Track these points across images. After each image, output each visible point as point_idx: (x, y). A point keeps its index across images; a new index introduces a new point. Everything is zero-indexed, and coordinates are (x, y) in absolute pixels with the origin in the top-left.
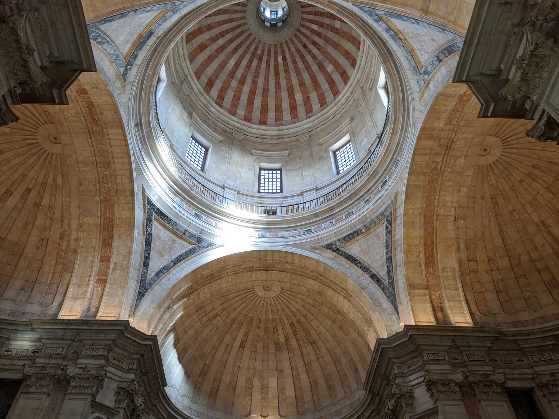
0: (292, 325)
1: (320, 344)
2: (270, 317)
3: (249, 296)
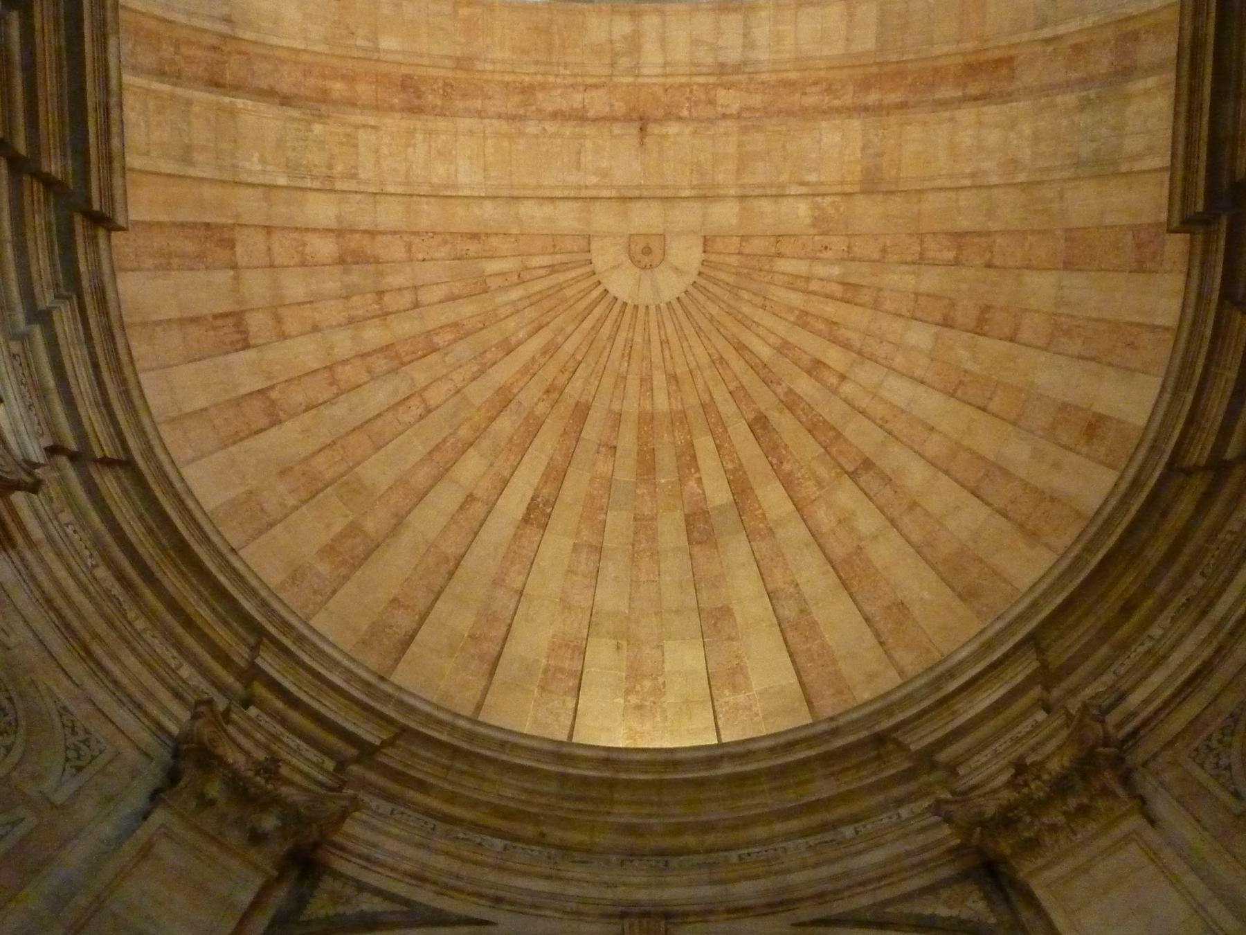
0: (760, 425)
1: (896, 458)
2: (662, 402)
3: (568, 292)
